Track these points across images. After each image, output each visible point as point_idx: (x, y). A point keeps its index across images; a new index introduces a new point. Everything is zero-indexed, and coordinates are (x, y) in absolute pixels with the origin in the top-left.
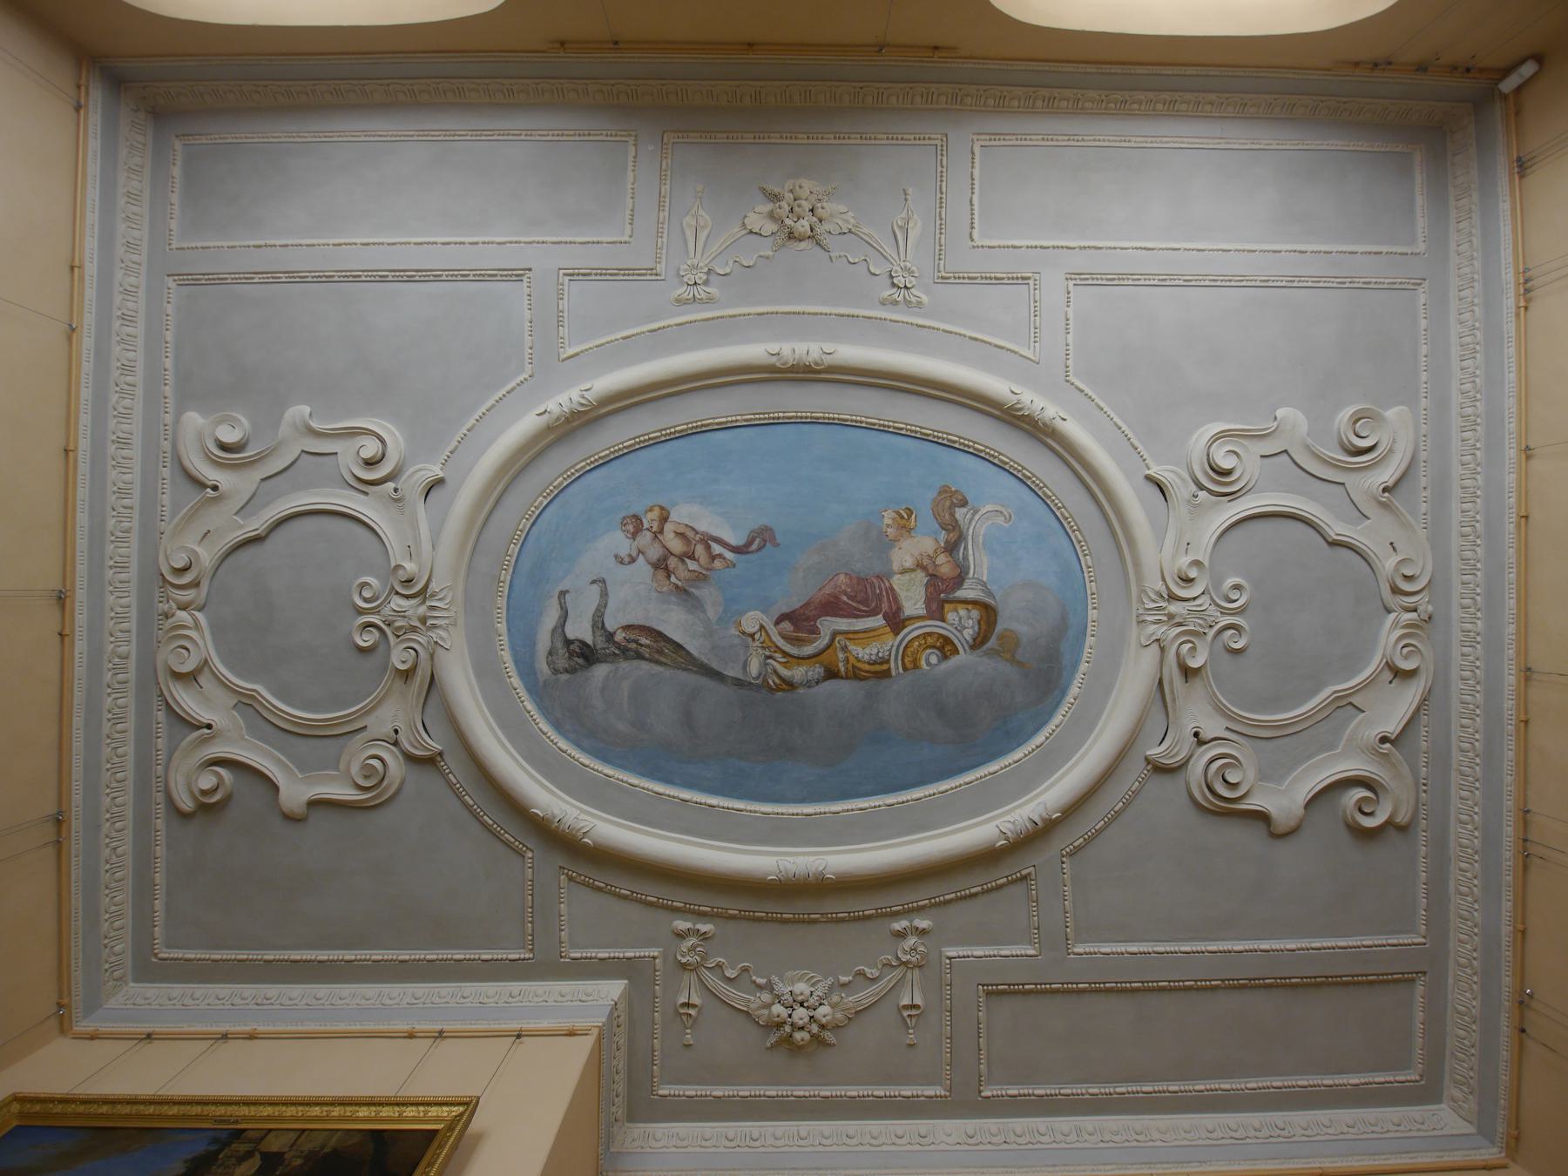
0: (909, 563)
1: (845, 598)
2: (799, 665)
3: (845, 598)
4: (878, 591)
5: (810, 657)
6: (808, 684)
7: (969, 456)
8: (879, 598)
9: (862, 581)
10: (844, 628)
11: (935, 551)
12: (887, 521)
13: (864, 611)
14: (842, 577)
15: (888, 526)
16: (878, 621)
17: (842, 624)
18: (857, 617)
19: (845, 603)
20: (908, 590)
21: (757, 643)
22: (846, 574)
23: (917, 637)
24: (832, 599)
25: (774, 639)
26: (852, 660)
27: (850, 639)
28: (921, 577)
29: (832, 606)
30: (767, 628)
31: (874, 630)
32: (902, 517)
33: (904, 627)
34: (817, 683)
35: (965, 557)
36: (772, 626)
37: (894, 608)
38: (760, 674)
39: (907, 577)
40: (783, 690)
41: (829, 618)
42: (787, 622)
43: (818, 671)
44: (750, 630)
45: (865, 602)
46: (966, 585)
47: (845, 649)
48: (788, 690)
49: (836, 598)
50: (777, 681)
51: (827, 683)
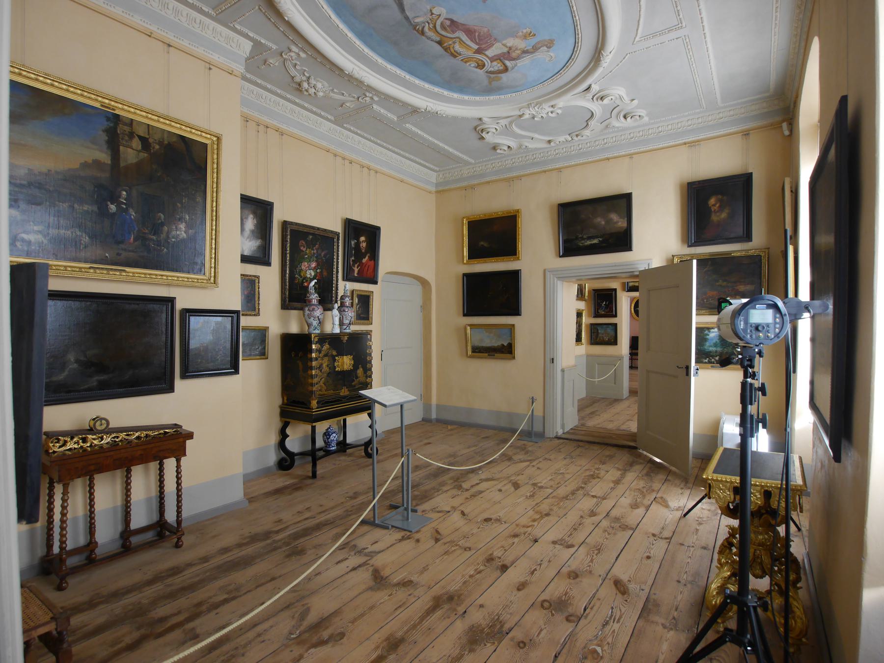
0: (508, 45)
1: (477, 34)
2: (434, 33)
3: (477, 34)
4: (489, 41)
5: (440, 34)
6: (429, 38)
7: (574, 40)
8: (487, 43)
9: (489, 36)
10: (463, 39)
11: (520, 49)
12: (525, 31)
13: (476, 42)
14: (487, 29)
15: (522, 32)
16: (476, 47)
17: (464, 38)
18: (472, 41)
19: (475, 35)
20: (496, 49)
21: (431, 17)
22: (489, 30)
23: (478, 58)
24: (473, 31)
25: (438, 21)
26: (452, 46)
27: (460, 43)
28: (505, 50)
29: (470, 32)
30: (440, 18)
31: (471, 47)
32: (529, 34)
33: (479, 54)
34: (431, 40)
35: (523, 57)
36: (443, 18)
37: (485, 48)
38: (417, 23)
39: (503, 46)
40: (418, 32)
41: (463, 33)
42: (450, 22)
43: (438, 39)
44: (434, 11)
45: (480, 40)
46: (511, 62)
47: (454, 43)
48: (420, 34)
49: (475, 31)
50: (420, 29)
51: (436, 43)
